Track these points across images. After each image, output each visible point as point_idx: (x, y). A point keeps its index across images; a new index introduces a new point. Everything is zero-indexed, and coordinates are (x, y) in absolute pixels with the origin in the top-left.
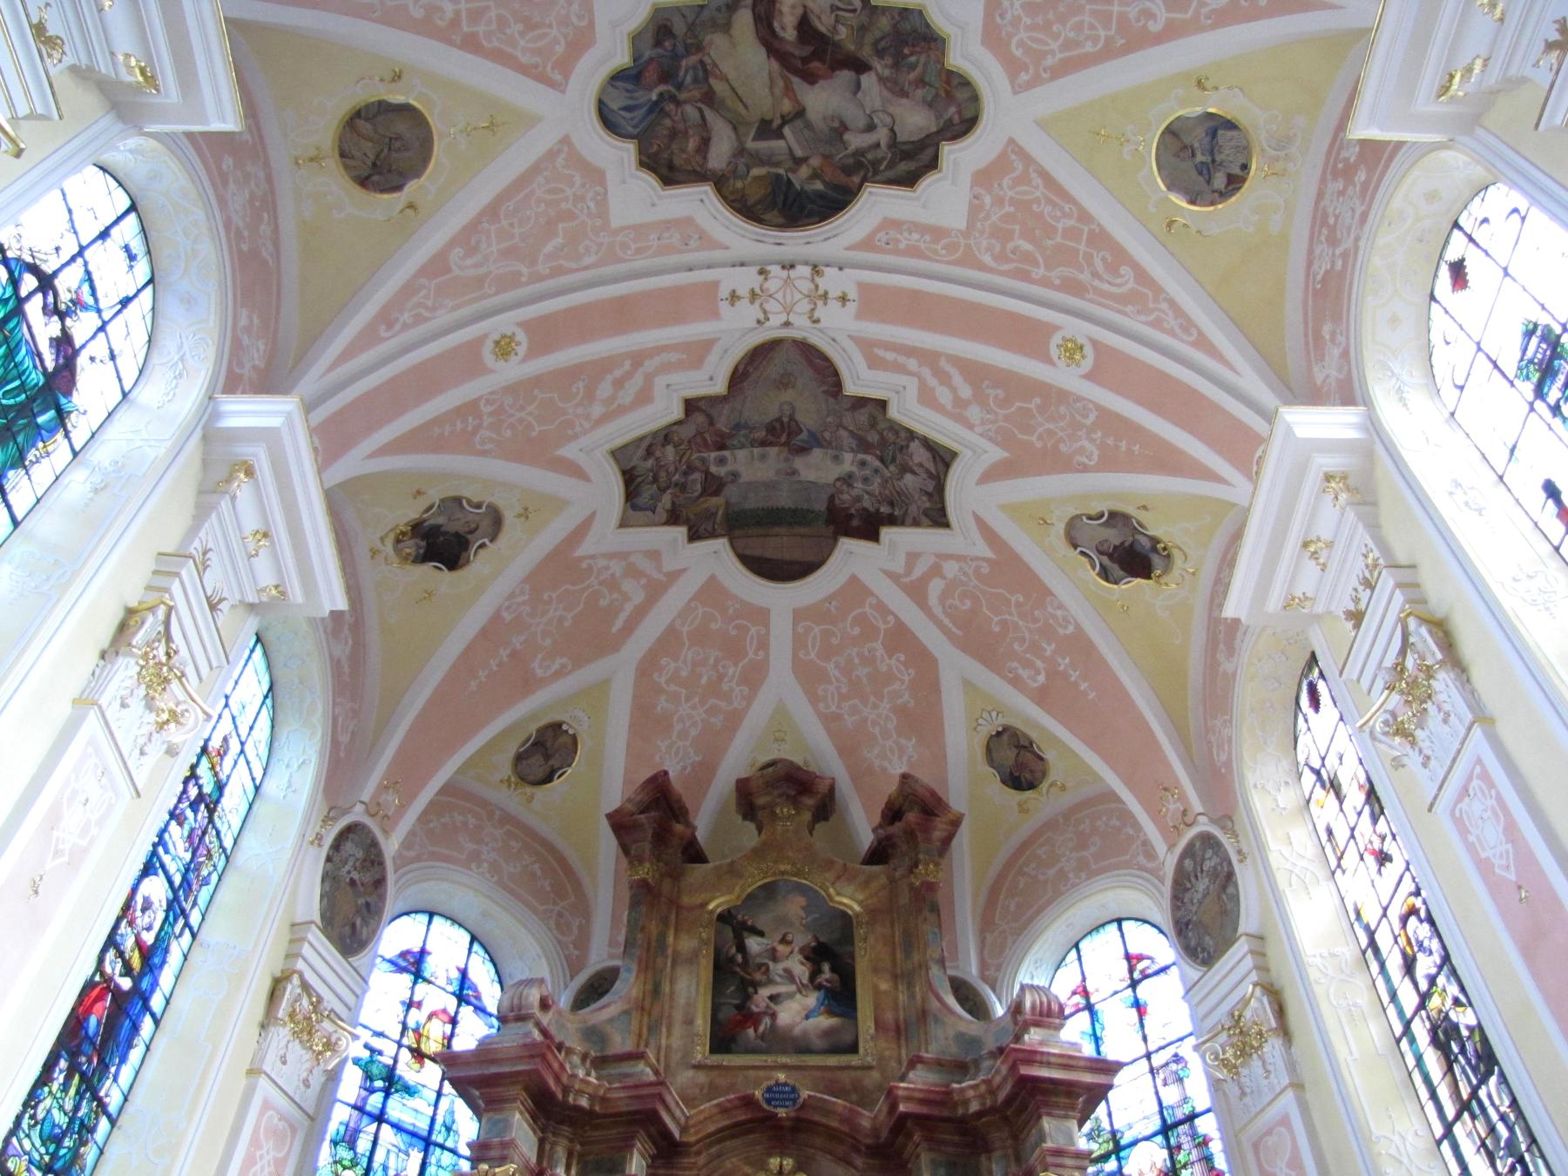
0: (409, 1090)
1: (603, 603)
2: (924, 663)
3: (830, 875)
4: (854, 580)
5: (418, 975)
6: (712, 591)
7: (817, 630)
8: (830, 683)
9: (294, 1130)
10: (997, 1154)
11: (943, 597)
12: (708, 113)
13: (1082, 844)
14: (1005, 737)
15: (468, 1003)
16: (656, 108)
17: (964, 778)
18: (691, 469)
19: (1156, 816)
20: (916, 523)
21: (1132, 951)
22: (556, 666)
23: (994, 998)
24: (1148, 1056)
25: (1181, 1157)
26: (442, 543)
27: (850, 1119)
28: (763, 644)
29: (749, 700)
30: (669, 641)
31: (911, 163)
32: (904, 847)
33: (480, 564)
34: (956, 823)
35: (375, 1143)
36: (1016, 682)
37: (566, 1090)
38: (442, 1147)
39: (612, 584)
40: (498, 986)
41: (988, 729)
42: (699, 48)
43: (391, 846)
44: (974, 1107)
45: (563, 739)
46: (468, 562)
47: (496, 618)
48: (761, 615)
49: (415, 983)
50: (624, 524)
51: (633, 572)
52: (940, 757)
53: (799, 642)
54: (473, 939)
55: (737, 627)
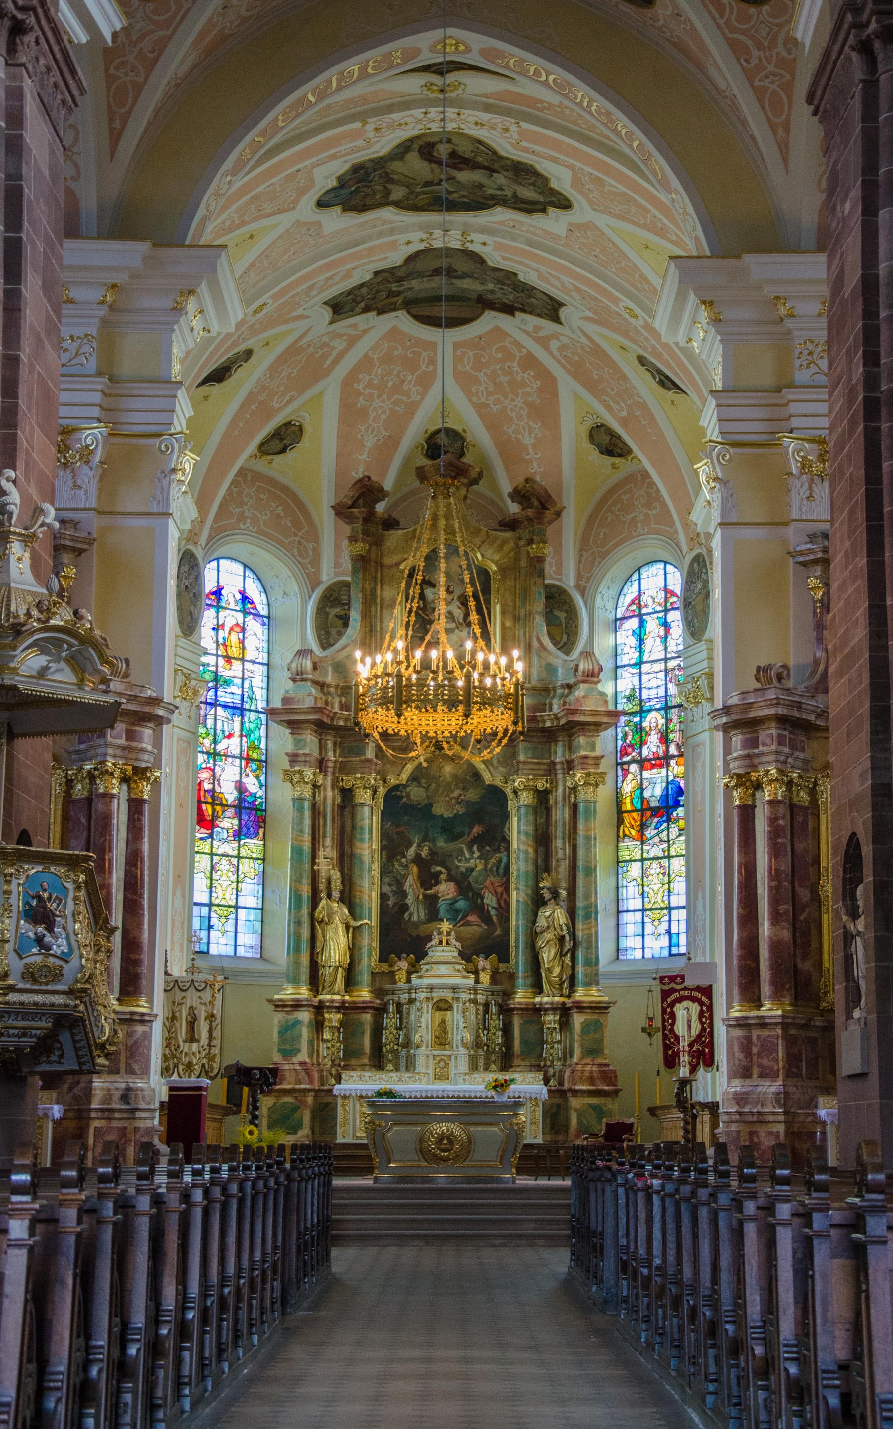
0: (228, 683)
1: (317, 356)
3: (477, 541)
4: (497, 328)
5: (219, 608)
7: (471, 353)
8: (480, 384)
9: (189, 743)
10: (560, 744)
12: (388, 185)
13: (649, 505)
14: (603, 429)
15: (250, 613)
16: (357, 191)
17: (569, 464)
18: (378, 291)
20: (539, 315)
21: (670, 588)
22: (288, 398)
23: (582, 604)
24: (666, 660)
25: (671, 726)
28: (432, 361)
29: (423, 396)
30: (365, 364)
32: (526, 523)
34: (558, 514)
35: (216, 719)
36: (608, 408)
37: (332, 719)
38: (250, 710)
39: (326, 344)
40: (263, 595)
41: (589, 424)
42: (383, 167)
44: (548, 724)
45: (292, 428)
46: (230, 375)
47: (251, 393)
48: (432, 346)
49: (218, 612)
50: (331, 323)
52: (556, 437)
53: (458, 360)
54: (245, 566)
55: (414, 352)
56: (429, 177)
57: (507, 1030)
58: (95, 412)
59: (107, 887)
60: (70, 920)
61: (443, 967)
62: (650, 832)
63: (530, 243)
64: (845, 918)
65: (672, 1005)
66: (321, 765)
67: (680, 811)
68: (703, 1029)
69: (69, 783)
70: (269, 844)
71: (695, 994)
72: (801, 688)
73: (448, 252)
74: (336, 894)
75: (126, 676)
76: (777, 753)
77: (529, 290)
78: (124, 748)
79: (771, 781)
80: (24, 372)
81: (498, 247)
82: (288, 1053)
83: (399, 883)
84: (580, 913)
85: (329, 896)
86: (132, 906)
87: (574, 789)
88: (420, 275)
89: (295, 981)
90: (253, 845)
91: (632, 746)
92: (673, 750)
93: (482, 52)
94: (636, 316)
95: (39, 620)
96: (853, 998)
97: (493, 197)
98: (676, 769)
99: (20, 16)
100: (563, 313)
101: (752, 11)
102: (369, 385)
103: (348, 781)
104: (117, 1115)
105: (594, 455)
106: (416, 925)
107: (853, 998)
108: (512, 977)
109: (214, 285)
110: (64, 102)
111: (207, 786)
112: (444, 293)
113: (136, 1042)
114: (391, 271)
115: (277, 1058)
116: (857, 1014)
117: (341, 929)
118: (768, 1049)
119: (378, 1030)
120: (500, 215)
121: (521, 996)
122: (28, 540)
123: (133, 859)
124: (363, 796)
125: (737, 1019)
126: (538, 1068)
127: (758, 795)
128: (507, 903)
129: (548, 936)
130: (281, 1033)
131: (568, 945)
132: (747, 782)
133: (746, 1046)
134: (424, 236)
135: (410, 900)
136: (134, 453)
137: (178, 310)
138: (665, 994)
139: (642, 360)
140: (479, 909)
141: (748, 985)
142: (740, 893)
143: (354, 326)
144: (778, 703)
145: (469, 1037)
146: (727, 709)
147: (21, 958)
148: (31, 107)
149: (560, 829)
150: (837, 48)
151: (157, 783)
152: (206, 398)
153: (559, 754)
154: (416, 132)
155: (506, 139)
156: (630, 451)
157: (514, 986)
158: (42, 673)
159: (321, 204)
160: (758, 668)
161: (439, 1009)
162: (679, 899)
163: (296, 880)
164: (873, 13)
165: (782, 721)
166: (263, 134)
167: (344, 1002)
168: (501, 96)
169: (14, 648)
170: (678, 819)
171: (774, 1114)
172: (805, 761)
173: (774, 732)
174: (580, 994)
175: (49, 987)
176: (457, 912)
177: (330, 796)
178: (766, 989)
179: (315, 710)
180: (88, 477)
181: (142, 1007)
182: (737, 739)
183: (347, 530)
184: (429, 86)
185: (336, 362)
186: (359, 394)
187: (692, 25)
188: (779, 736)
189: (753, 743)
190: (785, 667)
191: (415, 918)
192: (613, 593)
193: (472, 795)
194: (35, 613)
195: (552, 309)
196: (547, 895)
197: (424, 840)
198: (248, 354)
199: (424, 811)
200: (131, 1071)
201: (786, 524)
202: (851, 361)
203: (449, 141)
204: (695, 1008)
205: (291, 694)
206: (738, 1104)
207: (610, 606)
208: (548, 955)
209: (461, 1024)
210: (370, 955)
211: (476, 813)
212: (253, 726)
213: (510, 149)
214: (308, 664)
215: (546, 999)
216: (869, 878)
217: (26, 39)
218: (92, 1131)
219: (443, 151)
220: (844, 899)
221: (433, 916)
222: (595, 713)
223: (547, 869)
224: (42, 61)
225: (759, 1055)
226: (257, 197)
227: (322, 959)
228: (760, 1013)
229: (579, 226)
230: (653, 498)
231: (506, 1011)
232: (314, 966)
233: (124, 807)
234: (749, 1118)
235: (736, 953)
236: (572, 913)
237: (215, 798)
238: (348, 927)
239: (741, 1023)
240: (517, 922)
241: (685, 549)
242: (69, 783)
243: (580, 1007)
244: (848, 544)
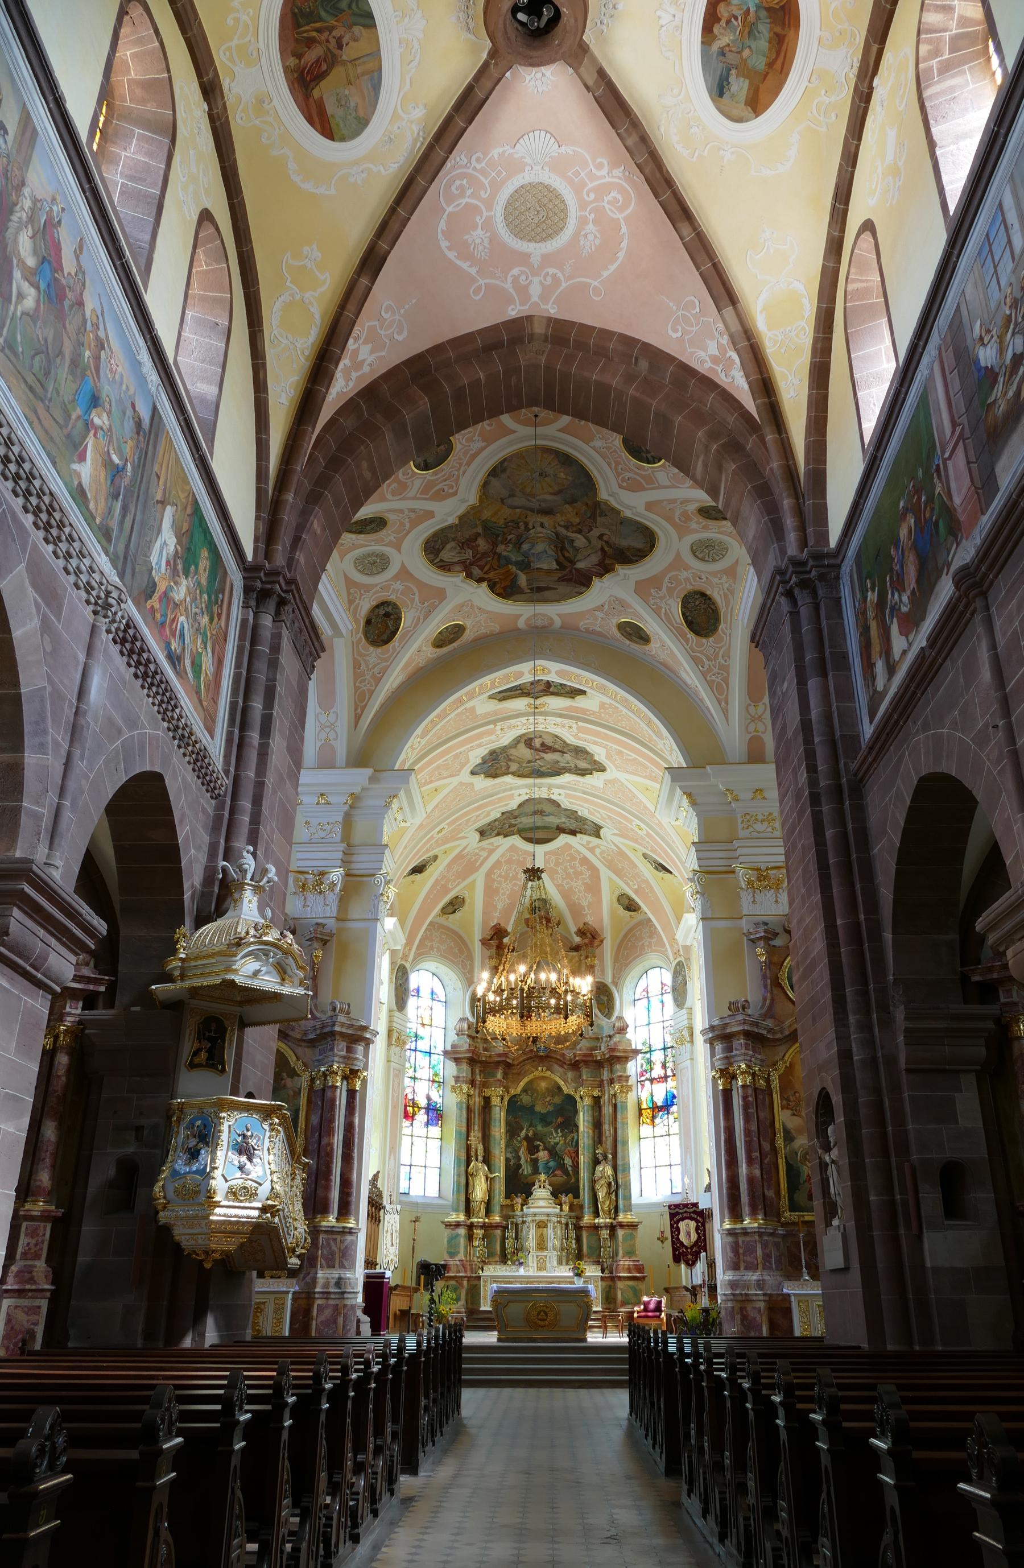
2: (595, 871)
6: (513, 848)
11: (601, 854)
13: (651, 937)
17: (605, 915)
19: (672, 946)
26: (418, 870)
27: (563, 1055)
30: (498, 864)
31: (583, 773)
33: (429, 870)
34: (602, 941)
36: (627, 884)
39: (477, 854)
41: (617, 894)
43: (408, 966)
51: (484, 849)
56: (530, 758)
57: (579, 1240)
58: (339, 863)
59: (331, 1145)
60: (265, 1152)
61: (541, 1202)
62: (657, 1121)
63: (584, 793)
64: (820, 1151)
65: (677, 1222)
66: (472, 1083)
67: (674, 1108)
68: (699, 1238)
69: (313, 1080)
70: (445, 1130)
71: (693, 1215)
72: (757, 1015)
73: (540, 800)
74: (480, 1158)
75: (348, 1013)
76: (746, 1054)
77: (583, 820)
78: (344, 1057)
79: (742, 1073)
80: (268, 792)
81: (567, 796)
82: (452, 1255)
83: (517, 1152)
84: (620, 1168)
85: (477, 1160)
86: (347, 1158)
87: (615, 1095)
88: (526, 815)
89: (456, 1210)
90: (435, 1131)
91: (646, 1071)
92: (669, 1073)
93: (557, 673)
94: (641, 829)
95: (255, 936)
96: (831, 1210)
97: (564, 768)
98: (671, 1083)
99: (283, 595)
100: (602, 832)
101: (704, 640)
102: (500, 875)
103: (487, 1092)
104: (332, 1296)
105: (621, 910)
106: (526, 1177)
107: (831, 1210)
108: (582, 1207)
109: (408, 792)
110: (311, 653)
111: (410, 1097)
112: (539, 824)
113: (346, 1247)
114: (511, 812)
115: (447, 1257)
116: (835, 1222)
117: (483, 1179)
118: (750, 1250)
119: (504, 1239)
120: (567, 778)
121: (587, 1219)
122: (257, 889)
123: (349, 1128)
124: (495, 1101)
125: (728, 1230)
126: (598, 1263)
127: (734, 1082)
128: (578, 1163)
129: (602, 1182)
130: (449, 1242)
131: (613, 1188)
132: (727, 1074)
133: (735, 1248)
134: (528, 791)
135: (522, 1162)
136: (358, 884)
137: (387, 806)
138: (672, 1216)
139: (645, 856)
140: (562, 1166)
141: (733, 1207)
142: (726, 1146)
143: (492, 844)
144: (745, 1022)
145: (557, 1244)
146: (712, 1028)
147: (226, 1181)
148: (286, 645)
149: (607, 1121)
150: (770, 601)
151: (364, 1081)
152: (413, 882)
153: (606, 1075)
154: (523, 731)
155: (569, 733)
156: (640, 908)
157: (582, 1213)
158: (256, 974)
159: (473, 773)
160: (730, 1003)
161: (539, 1227)
162: (677, 1159)
163: (457, 1151)
164: (793, 572)
165: (747, 1034)
166: (438, 716)
167: (485, 1223)
168: (567, 709)
169: (235, 956)
170: (673, 1113)
171: (756, 1295)
172: (762, 1060)
173: (742, 1041)
174: (621, 1218)
175: (247, 1204)
176: (549, 1168)
177: (477, 1101)
178: (746, 1209)
179: (469, 1051)
180: (332, 899)
181: (351, 1224)
182: (719, 1047)
183: (488, 953)
184: (529, 705)
185: (482, 864)
186: (494, 880)
187: (671, 651)
188: (746, 1044)
189: (729, 1049)
190: (746, 1001)
191: (525, 1172)
192: (633, 985)
193: (557, 1100)
194: (252, 932)
195: (596, 831)
196: (600, 1158)
197: (531, 1125)
198: (436, 858)
199: (530, 1109)
200: (342, 1266)
201: (741, 918)
202: (796, 774)
203: (541, 737)
204: (693, 1224)
205: (456, 1043)
206: (732, 1288)
207: (631, 993)
208: (601, 1194)
209: (554, 1236)
210: (500, 1194)
211: (559, 1111)
212: (436, 1063)
213: (573, 740)
214: (465, 1026)
215: (601, 1221)
216: (840, 1119)
217: (286, 608)
218: (315, 1307)
219: (537, 743)
220: (818, 1137)
221: (536, 1171)
222: (625, 1051)
223: (600, 1142)
224: (297, 624)
225: (744, 1255)
226: (438, 767)
227: (472, 1197)
228: (743, 1226)
229: (610, 781)
230: (653, 933)
231: (578, 1228)
232: (468, 1201)
233: (344, 1094)
234: (740, 1298)
235: (725, 1186)
236: (615, 1168)
237: (415, 1105)
238: (487, 1178)
239: (731, 1233)
240: (583, 1174)
241: (672, 959)
242: (313, 1080)
243: (621, 1225)
244: (803, 891)
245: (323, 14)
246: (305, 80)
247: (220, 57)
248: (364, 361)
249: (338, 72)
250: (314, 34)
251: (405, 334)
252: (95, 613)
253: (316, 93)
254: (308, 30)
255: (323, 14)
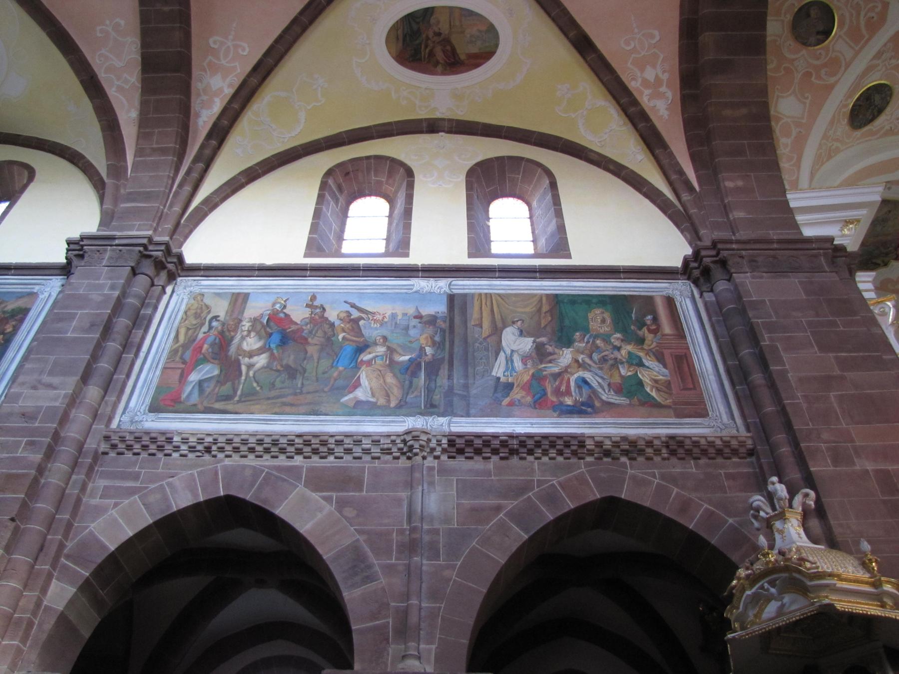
245: (417, 42)
246: (455, 63)
247: (422, 114)
248: (657, 76)
249: (455, 40)
250: (427, 50)
251: (656, 33)
252: (409, 458)
253: (463, 57)
254: (425, 53)
255: (417, 42)
